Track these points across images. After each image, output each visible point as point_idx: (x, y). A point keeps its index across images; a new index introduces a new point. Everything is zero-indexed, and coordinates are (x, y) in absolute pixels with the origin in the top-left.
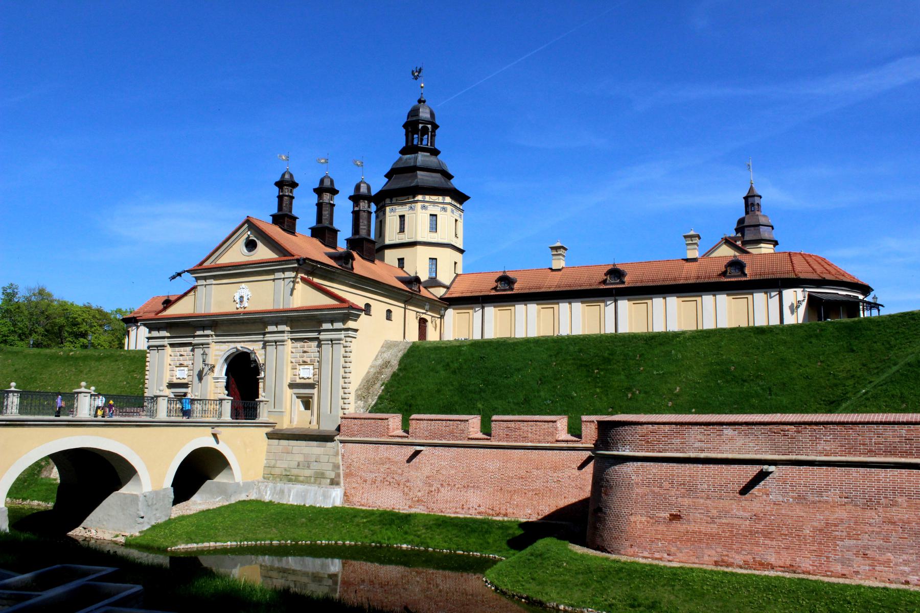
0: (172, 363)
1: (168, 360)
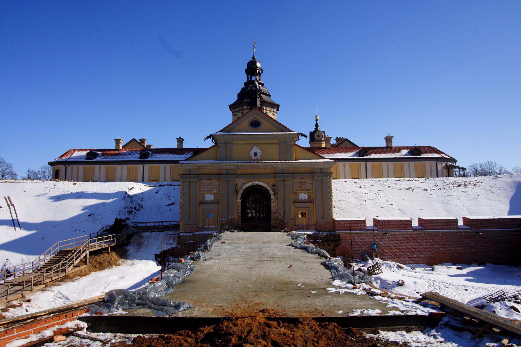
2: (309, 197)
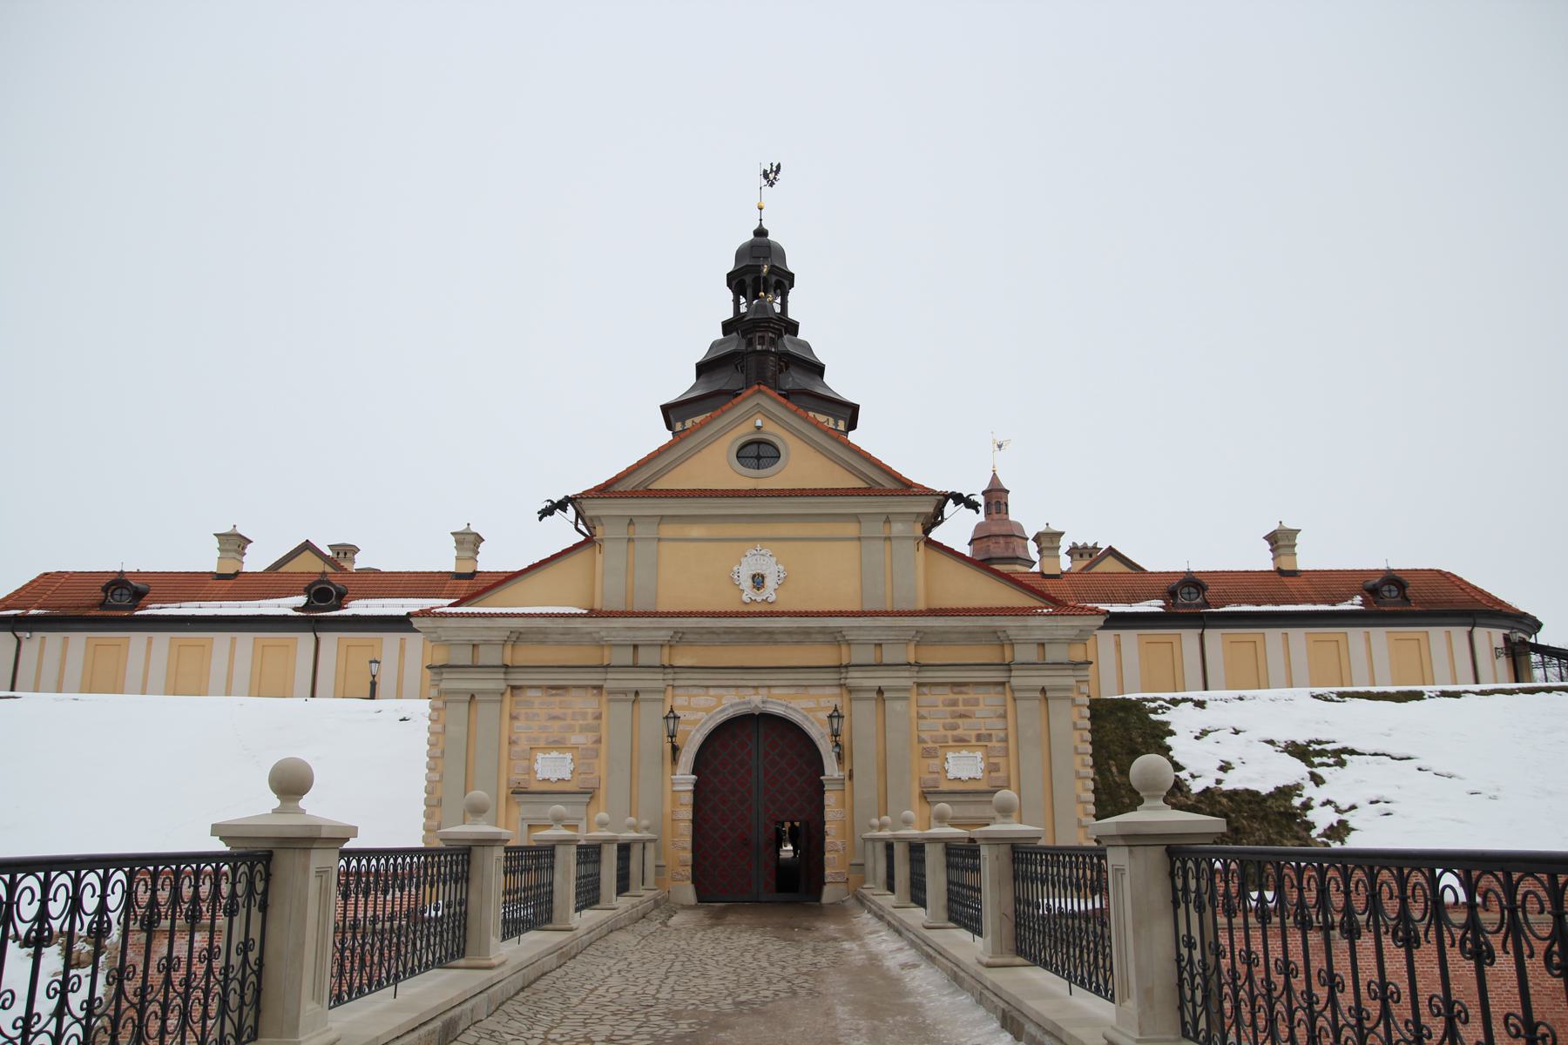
2: (992, 768)
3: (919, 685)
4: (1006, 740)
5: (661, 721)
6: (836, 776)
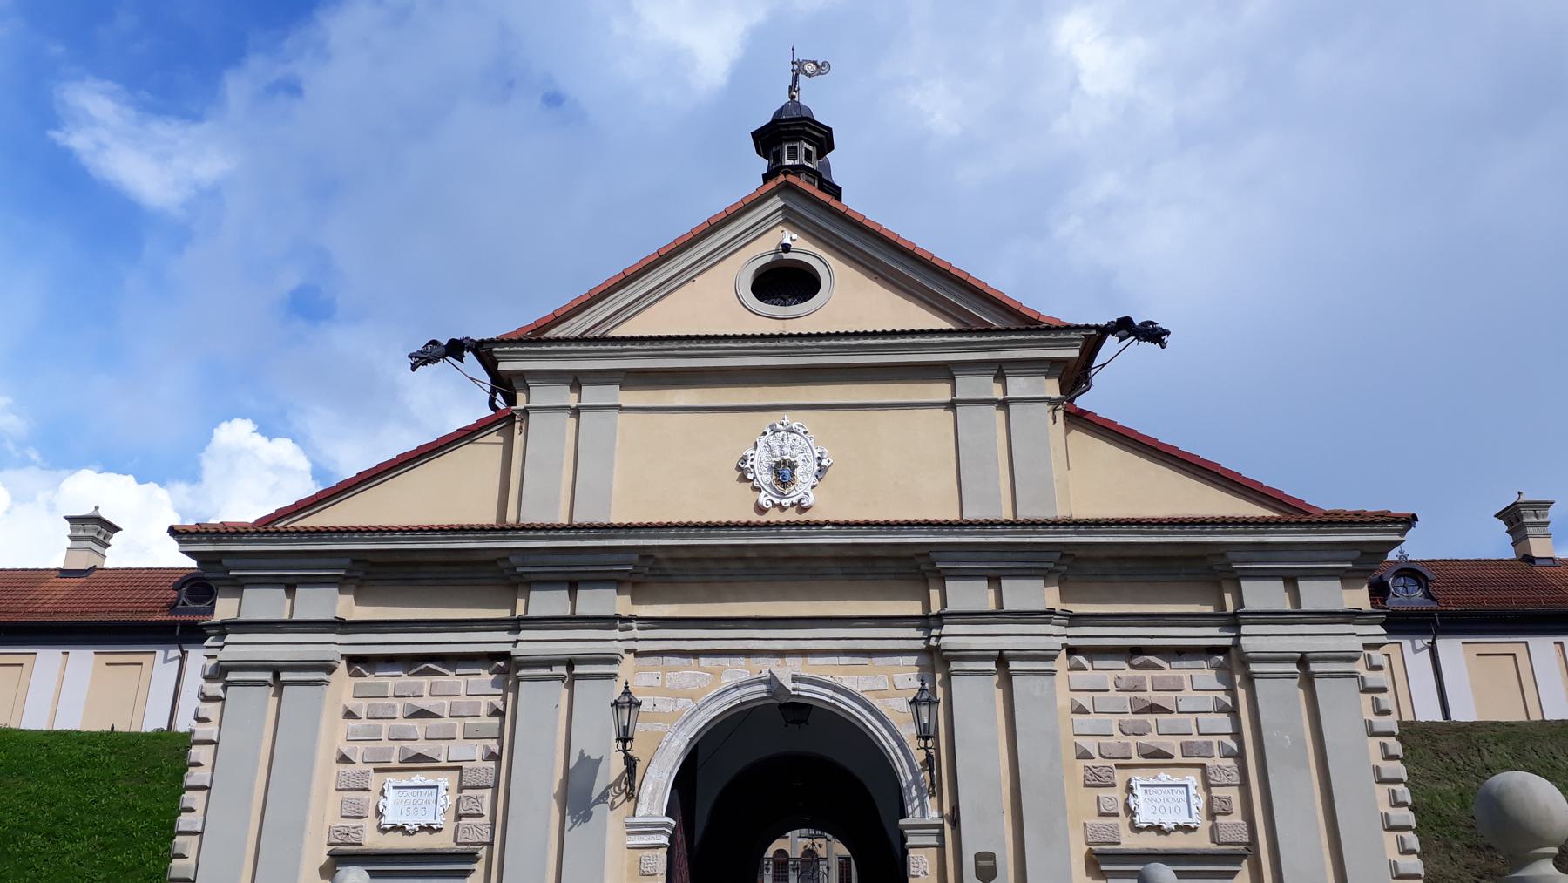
0: (358, 751)
1: (334, 734)
3: (1072, 651)
4: (1240, 756)
5: (609, 712)
6: (933, 815)
